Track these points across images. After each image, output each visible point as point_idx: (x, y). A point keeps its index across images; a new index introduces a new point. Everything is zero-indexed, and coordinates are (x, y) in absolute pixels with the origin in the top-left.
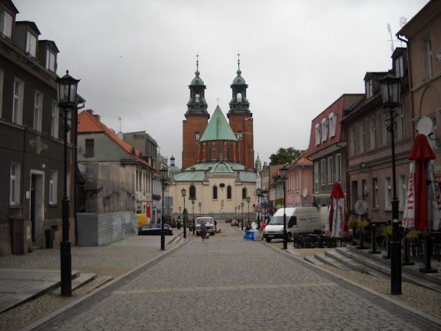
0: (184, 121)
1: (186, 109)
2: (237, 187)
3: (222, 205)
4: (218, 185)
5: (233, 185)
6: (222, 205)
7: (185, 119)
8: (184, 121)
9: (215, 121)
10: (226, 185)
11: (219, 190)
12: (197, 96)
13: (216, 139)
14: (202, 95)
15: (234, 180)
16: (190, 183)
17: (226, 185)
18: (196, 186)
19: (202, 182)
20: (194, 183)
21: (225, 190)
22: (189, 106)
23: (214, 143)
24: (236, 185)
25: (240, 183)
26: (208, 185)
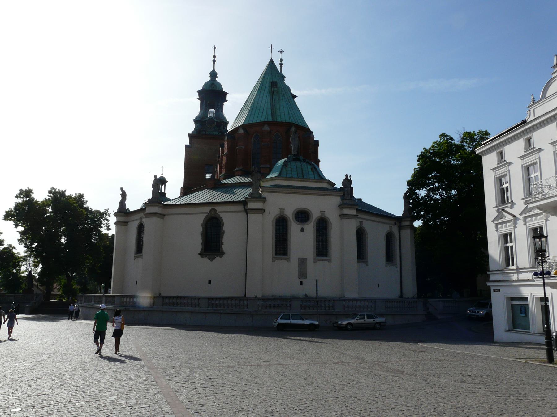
0: (186, 146)
1: (191, 127)
2: (346, 221)
3: (302, 274)
4: (290, 214)
5: (332, 216)
6: (302, 274)
7: (189, 144)
8: (186, 146)
9: (268, 84)
10: (315, 215)
11: (294, 228)
12: (212, 111)
13: (270, 119)
14: (219, 109)
15: (337, 200)
16: (207, 209)
17: (315, 215)
18: (222, 215)
19: (244, 203)
20: (219, 209)
21: (310, 228)
22: (196, 121)
23: (266, 128)
24: (342, 216)
25: (353, 212)
26: (262, 211)
